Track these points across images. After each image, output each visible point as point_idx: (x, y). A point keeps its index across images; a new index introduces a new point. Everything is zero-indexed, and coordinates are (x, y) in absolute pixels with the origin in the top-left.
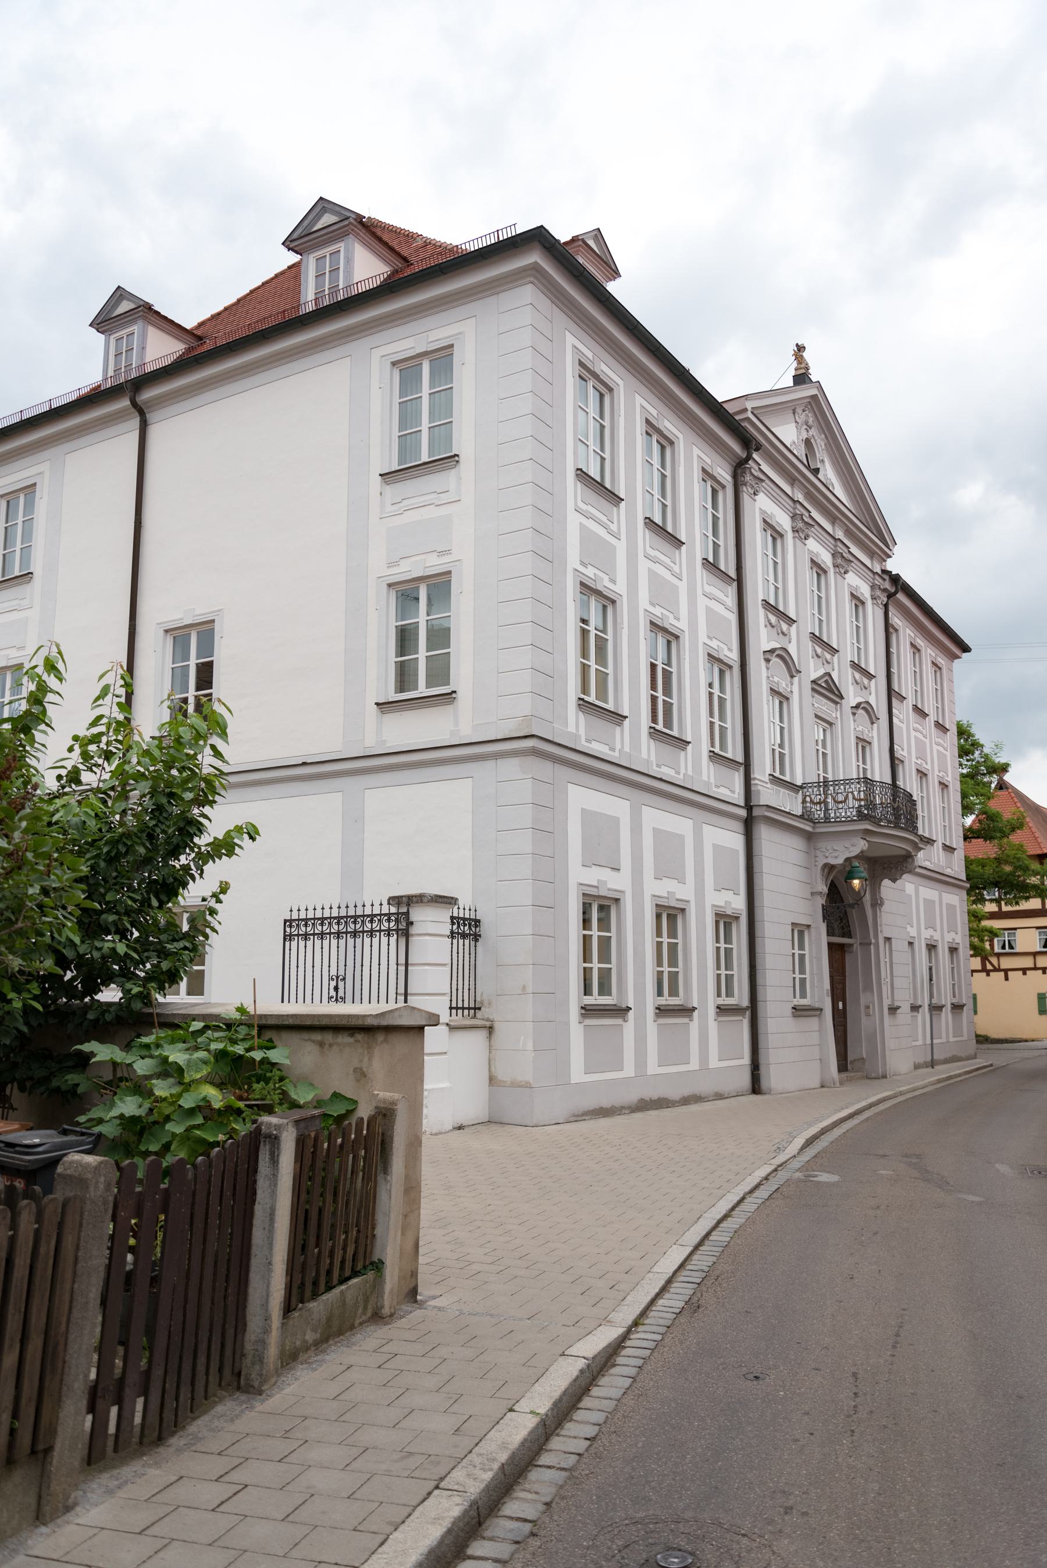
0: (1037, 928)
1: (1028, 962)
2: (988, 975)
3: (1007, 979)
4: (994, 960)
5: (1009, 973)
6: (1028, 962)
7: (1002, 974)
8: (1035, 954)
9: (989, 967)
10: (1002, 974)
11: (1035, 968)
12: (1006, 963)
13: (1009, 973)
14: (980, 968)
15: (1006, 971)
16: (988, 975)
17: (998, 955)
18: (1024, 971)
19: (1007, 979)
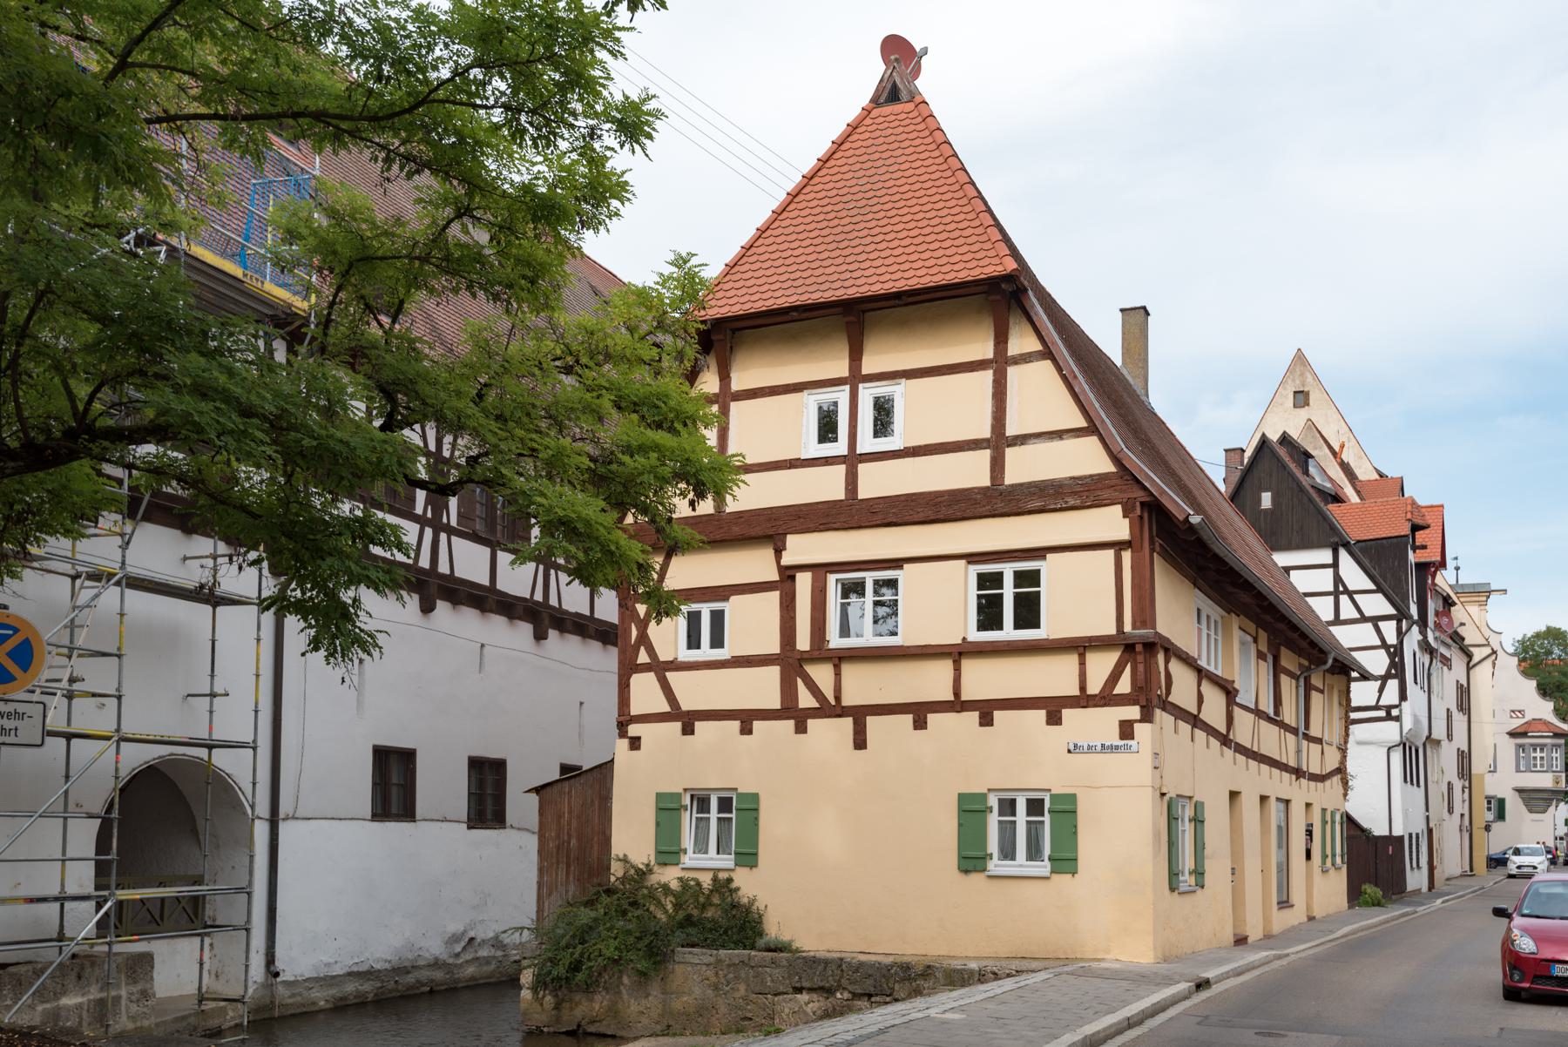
0: (972, 558)
1: (933, 681)
2: (801, 728)
3: (860, 742)
4: (822, 674)
5: (872, 722)
6: (933, 681)
7: (847, 723)
8: (959, 653)
9: (806, 700)
10: (847, 723)
11: (958, 705)
12: (861, 685)
13: (872, 722)
14: (775, 704)
15: (860, 715)
16: (801, 728)
17: (840, 659)
18: (920, 713)
19: (860, 742)
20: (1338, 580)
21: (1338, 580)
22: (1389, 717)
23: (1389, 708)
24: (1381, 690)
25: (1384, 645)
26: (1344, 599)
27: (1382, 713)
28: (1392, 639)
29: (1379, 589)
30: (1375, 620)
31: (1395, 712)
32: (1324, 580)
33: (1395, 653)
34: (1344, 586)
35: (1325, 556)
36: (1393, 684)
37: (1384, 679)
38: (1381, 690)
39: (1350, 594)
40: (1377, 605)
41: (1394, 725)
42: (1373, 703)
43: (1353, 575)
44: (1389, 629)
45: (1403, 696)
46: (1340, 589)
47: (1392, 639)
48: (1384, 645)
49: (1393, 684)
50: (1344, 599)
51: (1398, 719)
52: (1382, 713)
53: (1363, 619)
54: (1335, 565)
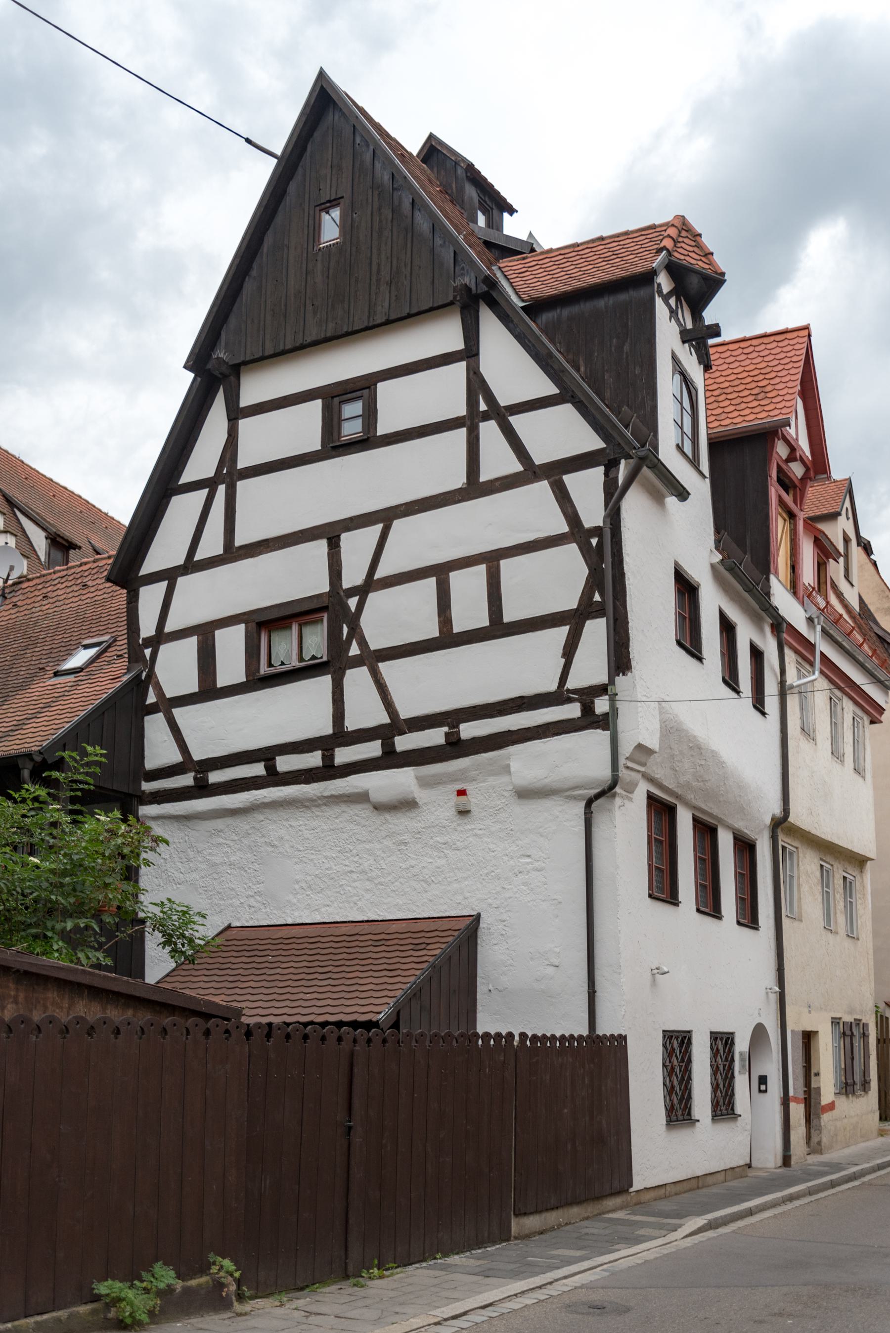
20: (477, 385)
21: (477, 385)
22: (590, 720)
23: (587, 695)
24: (569, 651)
25: (577, 532)
26: (489, 430)
27: (573, 711)
28: (592, 514)
29: (566, 395)
30: (555, 473)
31: (601, 705)
32: (446, 392)
33: (603, 551)
34: (490, 399)
35: (445, 335)
36: (596, 631)
37: (574, 620)
38: (569, 651)
39: (502, 415)
40: (560, 432)
41: (595, 741)
42: (552, 686)
43: (509, 368)
44: (587, 488)
45: (620, 660)
46: (484, 407)
47: (592, 514)
48: (577, 532)
49: (596, 631)
50: (489, 430)
51: (606, 722)
52: (573, 711)
53: (531, 472)
54: (470, 353)
